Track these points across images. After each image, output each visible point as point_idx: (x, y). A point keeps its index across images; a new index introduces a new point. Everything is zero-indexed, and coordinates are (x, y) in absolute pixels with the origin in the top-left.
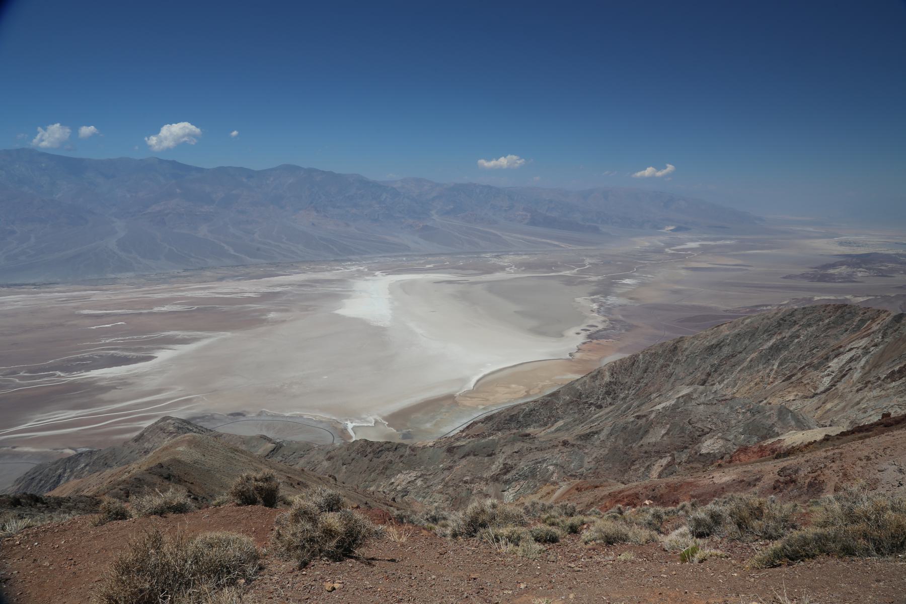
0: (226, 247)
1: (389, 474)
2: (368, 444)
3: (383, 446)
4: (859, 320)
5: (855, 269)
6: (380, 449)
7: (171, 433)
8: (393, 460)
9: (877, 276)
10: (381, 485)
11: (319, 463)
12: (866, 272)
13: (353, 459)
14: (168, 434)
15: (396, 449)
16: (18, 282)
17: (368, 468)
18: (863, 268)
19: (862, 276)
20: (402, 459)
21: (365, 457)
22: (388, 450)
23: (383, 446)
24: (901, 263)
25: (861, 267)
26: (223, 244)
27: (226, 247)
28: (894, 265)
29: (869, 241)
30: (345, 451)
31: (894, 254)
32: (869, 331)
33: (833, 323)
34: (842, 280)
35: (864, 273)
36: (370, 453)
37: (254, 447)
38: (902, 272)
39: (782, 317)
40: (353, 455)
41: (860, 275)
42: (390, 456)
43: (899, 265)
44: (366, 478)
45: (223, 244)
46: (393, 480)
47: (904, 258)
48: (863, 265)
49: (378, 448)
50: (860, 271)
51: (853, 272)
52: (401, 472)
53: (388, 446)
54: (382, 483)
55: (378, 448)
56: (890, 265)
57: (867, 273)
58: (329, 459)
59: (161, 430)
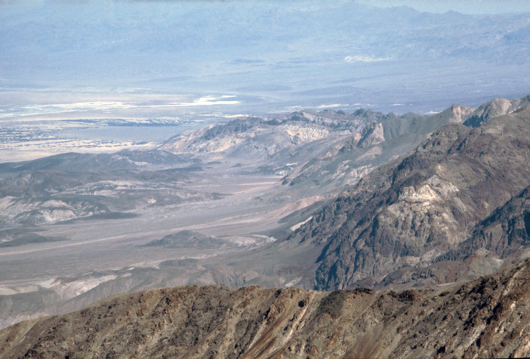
4: (239, 325)
5: (37, 204)
9: (95, 217)
12: (63, 208)
18: (57, 199)
19: (59, 223)
24: (143, 177)
25: (48, 197)
28: (129, 183)
29: (45, 122)
31: (119, 153)
32: (272, 350)
33: (173, 342)
34: (11, 239)
35: (61, 212)
38: (153, 201)
39: (29, 346)
41: (49, 218)
43: (139, 183)
47: (144, 163)
48: (52, 190)
50: (52, 209)
51: (34, 212)
56: (121, 184)
57: (70, 213)
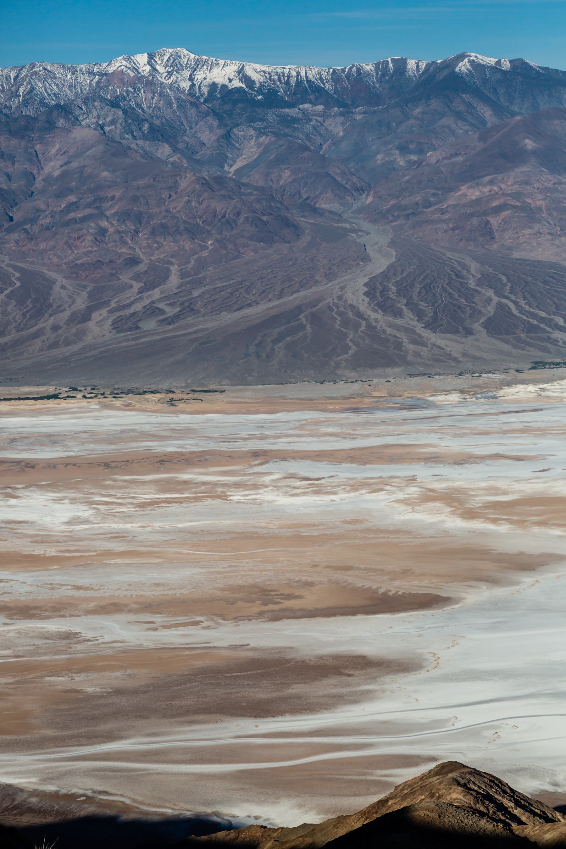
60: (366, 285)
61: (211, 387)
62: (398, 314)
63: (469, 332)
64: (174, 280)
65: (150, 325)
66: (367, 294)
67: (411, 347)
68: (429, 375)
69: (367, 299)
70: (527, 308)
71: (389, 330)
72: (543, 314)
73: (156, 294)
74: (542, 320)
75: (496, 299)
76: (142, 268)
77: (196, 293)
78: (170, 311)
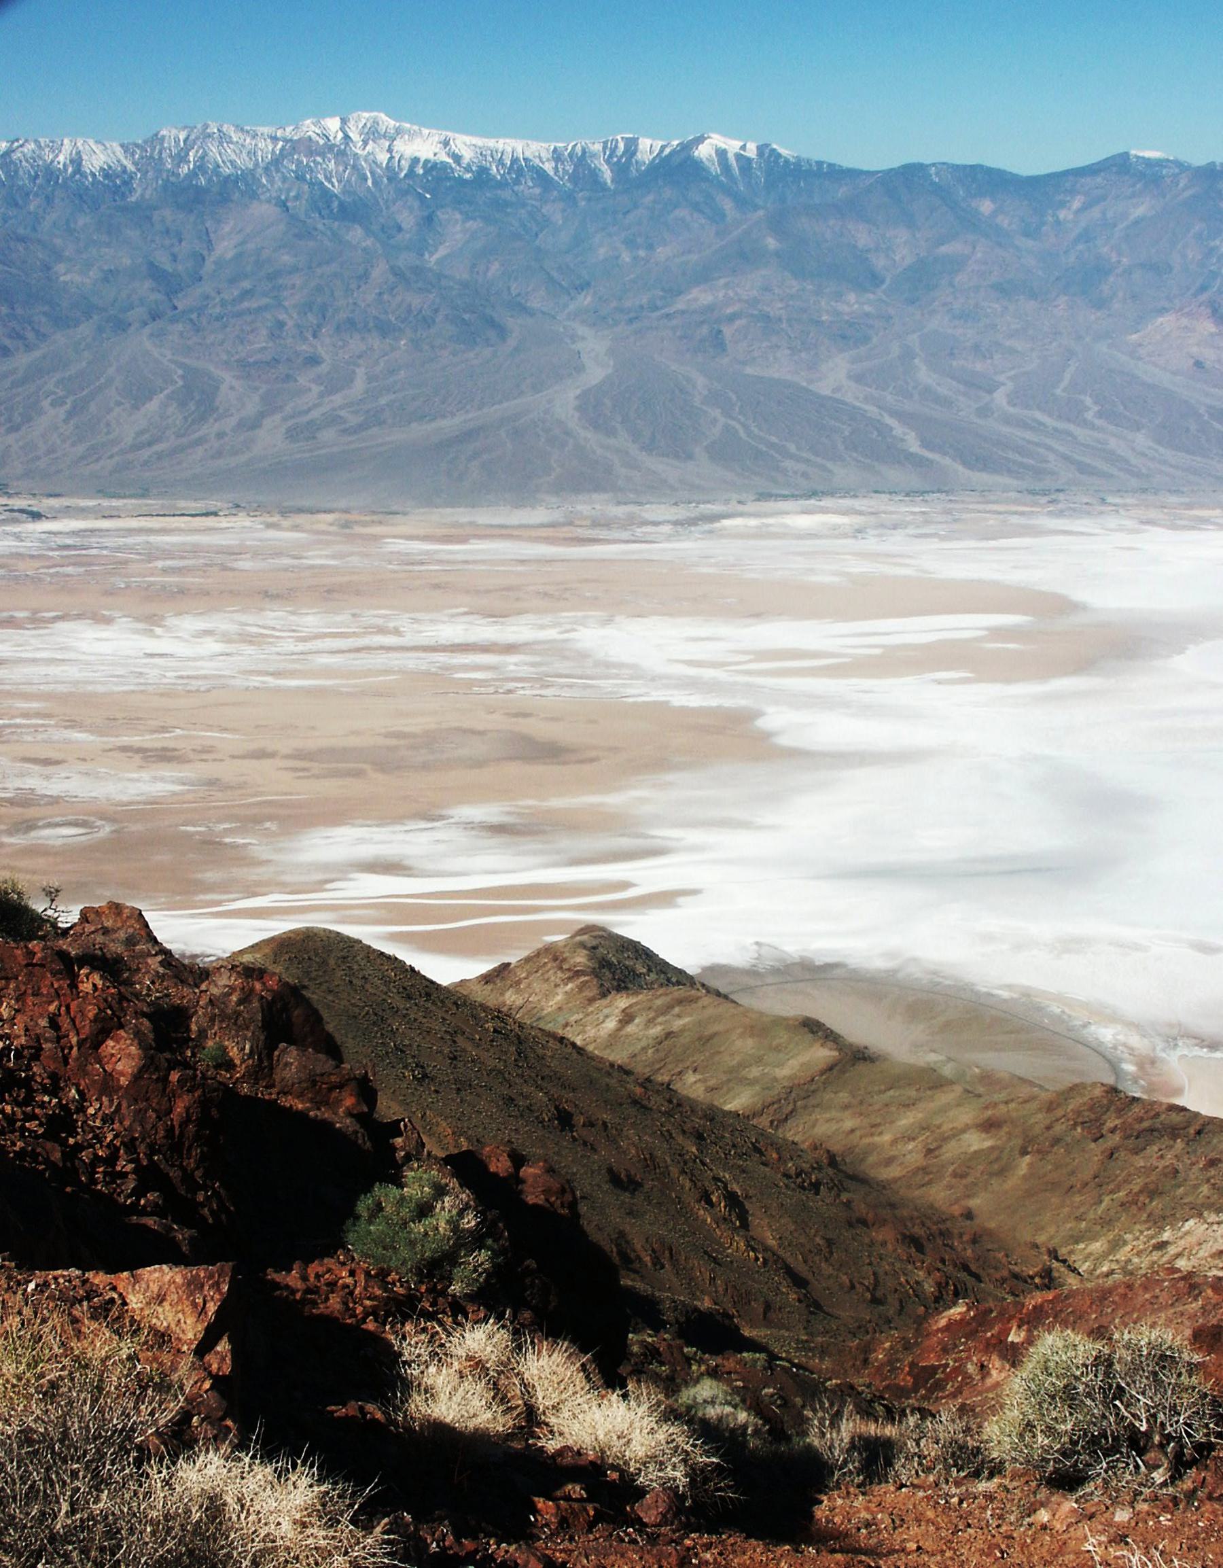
0: (898, 429)
1: (1157, 1212)
2: (1111, 1102)
3: (1157, 1115)
6: (1146, 1124)
7: (578, 974)
8: (1180, 1167)
10: (1125, 1243)
11: (957, 1133)
13: (1057, 1141)
14: (568, 974)
15: (1199, 1133)
16: (307, 503)
17: (1095, 1177)
20: (1213, 1172)
21: (1095, 1140)
22: (1174, 1132)
23: (1157, 1115)
26: (889, 420)
27: (898, 429)
30: (1040, 1110)
36: (1113, 1131)
37: (777, 1049)
40: (1059, 1128)
42: (1168, 1154)
44: (1082, 1210)
45: (889, 420)
46: (1166, 1236)
49: (1141, 1120)
52: (1200, 1215)
53: (1176, 1118)
54: (1128, 1237)
55: (1141, 1120)
58: (989, 1126)
59: (555, 959)
60: (577, 398)
61: (395, 508)
62: (611, 432)
63: (690, 457)
64: (359, 385)
65: (328, 435)
66: (578, 408)
67: (623, 471)
68: (640, 504)
69: (577, 415)
70: (756, 431)
71: (599, 451)
72: (774, 439)
73: (338, 399)
74: (772, 445)
75: (722, 420)
76: (323, 368)
77: (383, 401)
78: (354, 420)
